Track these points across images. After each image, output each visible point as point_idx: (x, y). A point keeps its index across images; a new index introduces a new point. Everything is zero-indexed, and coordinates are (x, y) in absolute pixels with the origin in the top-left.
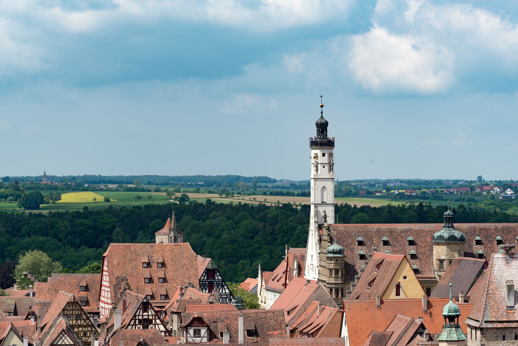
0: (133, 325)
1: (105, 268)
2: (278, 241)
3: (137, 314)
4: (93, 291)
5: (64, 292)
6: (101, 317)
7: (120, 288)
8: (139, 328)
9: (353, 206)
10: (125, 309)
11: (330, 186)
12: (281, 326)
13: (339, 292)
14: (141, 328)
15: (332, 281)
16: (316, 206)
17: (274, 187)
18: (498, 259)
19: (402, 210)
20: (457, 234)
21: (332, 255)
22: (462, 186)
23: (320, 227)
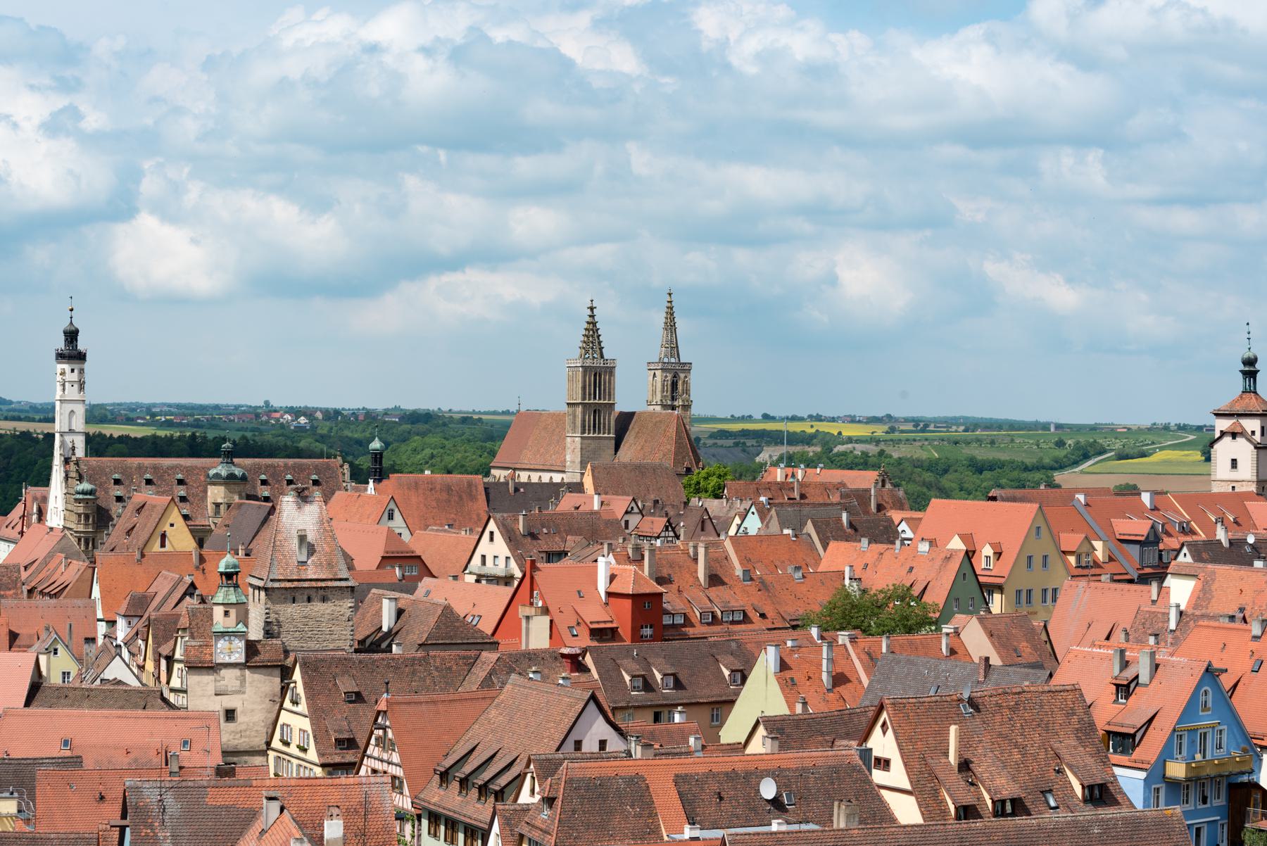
11: (80, 410)
13: (89, 543)
15: (81, 528)
16: (62, 434)
17: (9, 410)
18: (288, 502)
19: (170, 440)
20: (238, 472)
21: (81, 497)
22: (244, 412)
23: (67, 461)
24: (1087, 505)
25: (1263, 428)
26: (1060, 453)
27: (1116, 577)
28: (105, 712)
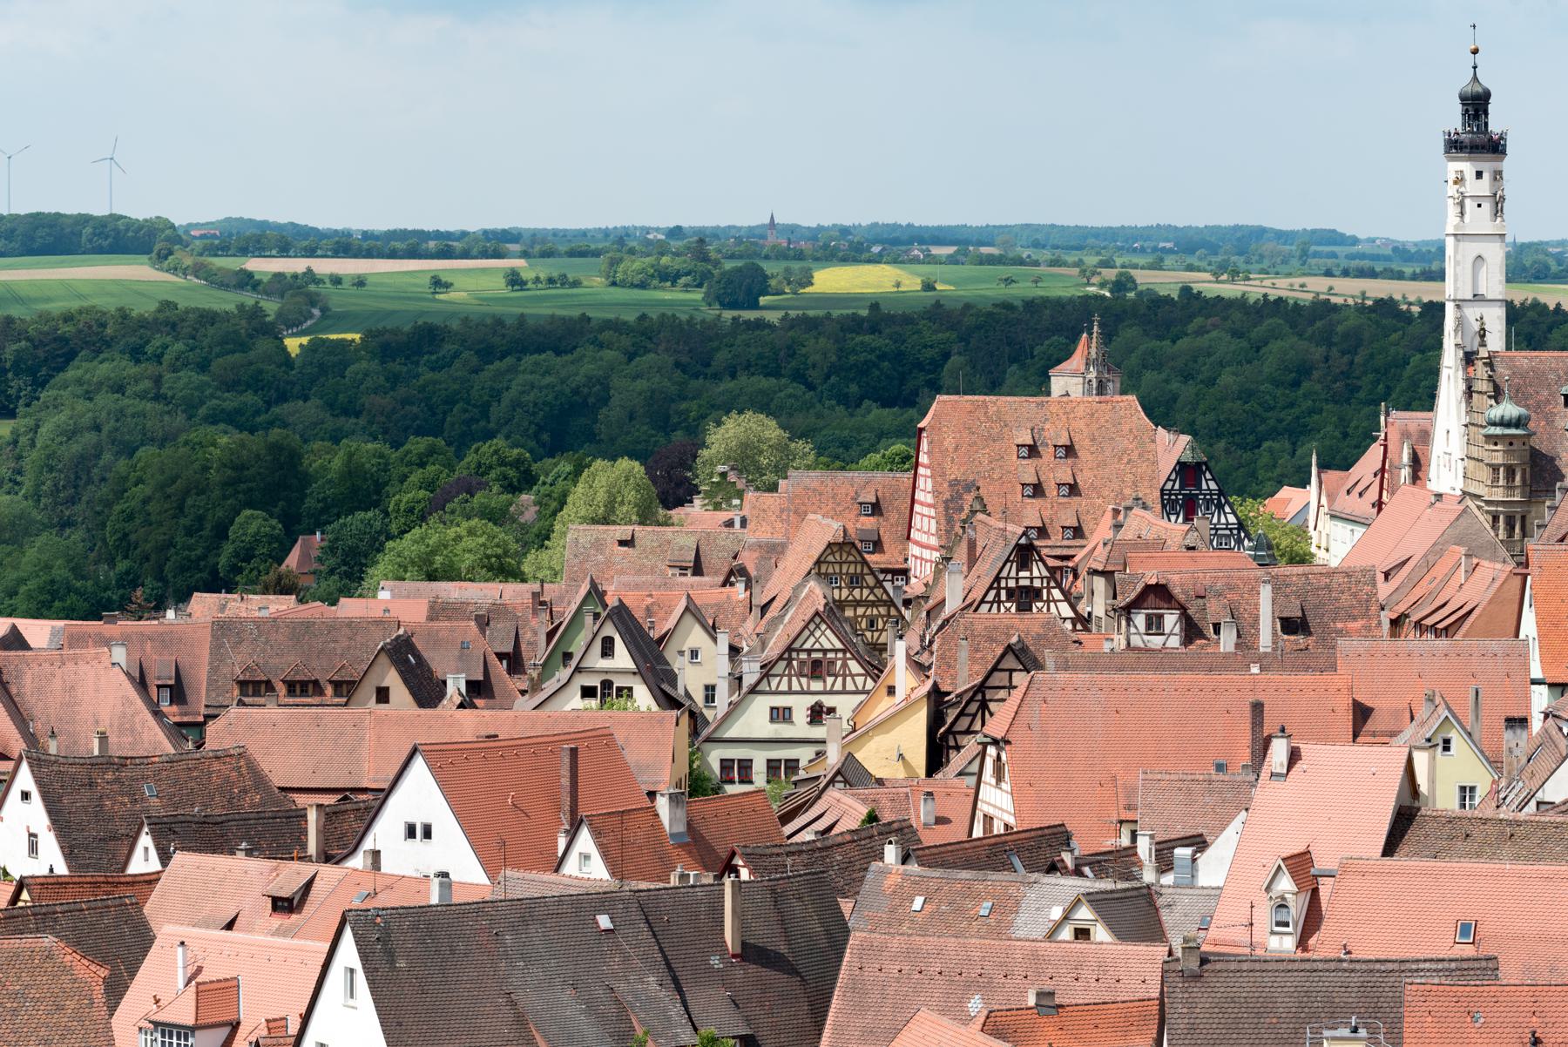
0: (992, 603)
1: (923, 459)
2: (1362, 395)
3: (1004, 574)
4: (893, 517)
5: (819, 517)
6: (913, 580)
7: (962, 509)
8: (1008, 610)
9: (1552, 307)
10: (972, 560)
11: (1495, 256)
12: (1368, 609)
14: (1013, 610)
15: (1499, 495)
21: (1498, 431)
23: (1469, 359)
28: (1544, 868)
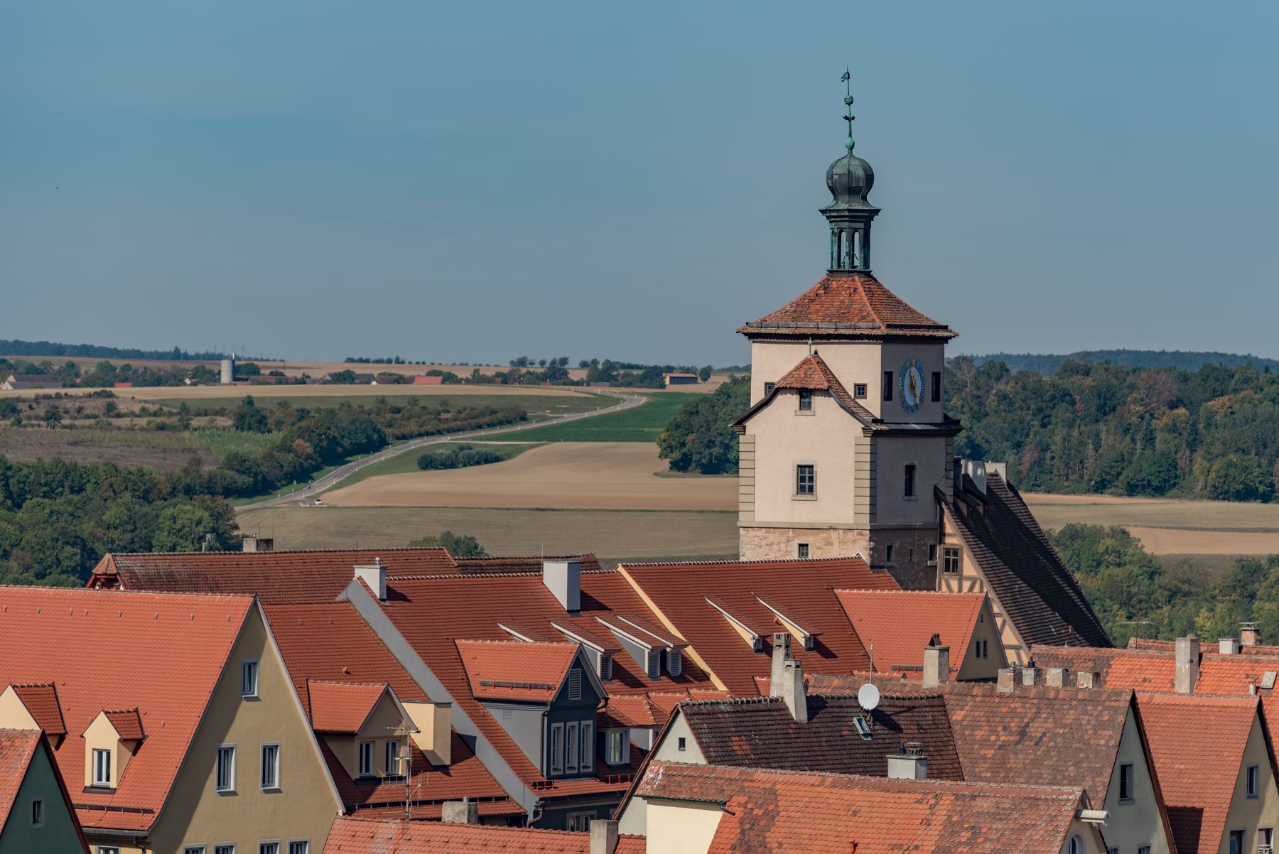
24: (391, 594)
25: (888, 377)
26: (253, 445)
27: (485, 809)
